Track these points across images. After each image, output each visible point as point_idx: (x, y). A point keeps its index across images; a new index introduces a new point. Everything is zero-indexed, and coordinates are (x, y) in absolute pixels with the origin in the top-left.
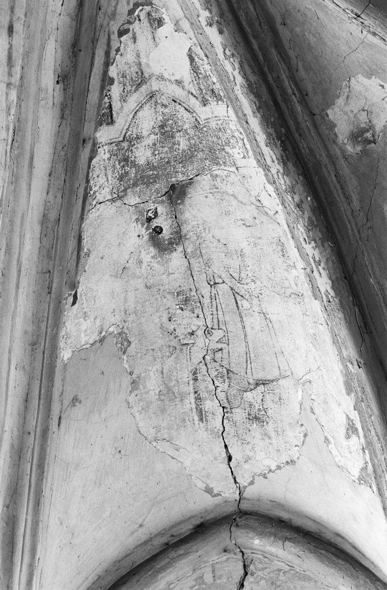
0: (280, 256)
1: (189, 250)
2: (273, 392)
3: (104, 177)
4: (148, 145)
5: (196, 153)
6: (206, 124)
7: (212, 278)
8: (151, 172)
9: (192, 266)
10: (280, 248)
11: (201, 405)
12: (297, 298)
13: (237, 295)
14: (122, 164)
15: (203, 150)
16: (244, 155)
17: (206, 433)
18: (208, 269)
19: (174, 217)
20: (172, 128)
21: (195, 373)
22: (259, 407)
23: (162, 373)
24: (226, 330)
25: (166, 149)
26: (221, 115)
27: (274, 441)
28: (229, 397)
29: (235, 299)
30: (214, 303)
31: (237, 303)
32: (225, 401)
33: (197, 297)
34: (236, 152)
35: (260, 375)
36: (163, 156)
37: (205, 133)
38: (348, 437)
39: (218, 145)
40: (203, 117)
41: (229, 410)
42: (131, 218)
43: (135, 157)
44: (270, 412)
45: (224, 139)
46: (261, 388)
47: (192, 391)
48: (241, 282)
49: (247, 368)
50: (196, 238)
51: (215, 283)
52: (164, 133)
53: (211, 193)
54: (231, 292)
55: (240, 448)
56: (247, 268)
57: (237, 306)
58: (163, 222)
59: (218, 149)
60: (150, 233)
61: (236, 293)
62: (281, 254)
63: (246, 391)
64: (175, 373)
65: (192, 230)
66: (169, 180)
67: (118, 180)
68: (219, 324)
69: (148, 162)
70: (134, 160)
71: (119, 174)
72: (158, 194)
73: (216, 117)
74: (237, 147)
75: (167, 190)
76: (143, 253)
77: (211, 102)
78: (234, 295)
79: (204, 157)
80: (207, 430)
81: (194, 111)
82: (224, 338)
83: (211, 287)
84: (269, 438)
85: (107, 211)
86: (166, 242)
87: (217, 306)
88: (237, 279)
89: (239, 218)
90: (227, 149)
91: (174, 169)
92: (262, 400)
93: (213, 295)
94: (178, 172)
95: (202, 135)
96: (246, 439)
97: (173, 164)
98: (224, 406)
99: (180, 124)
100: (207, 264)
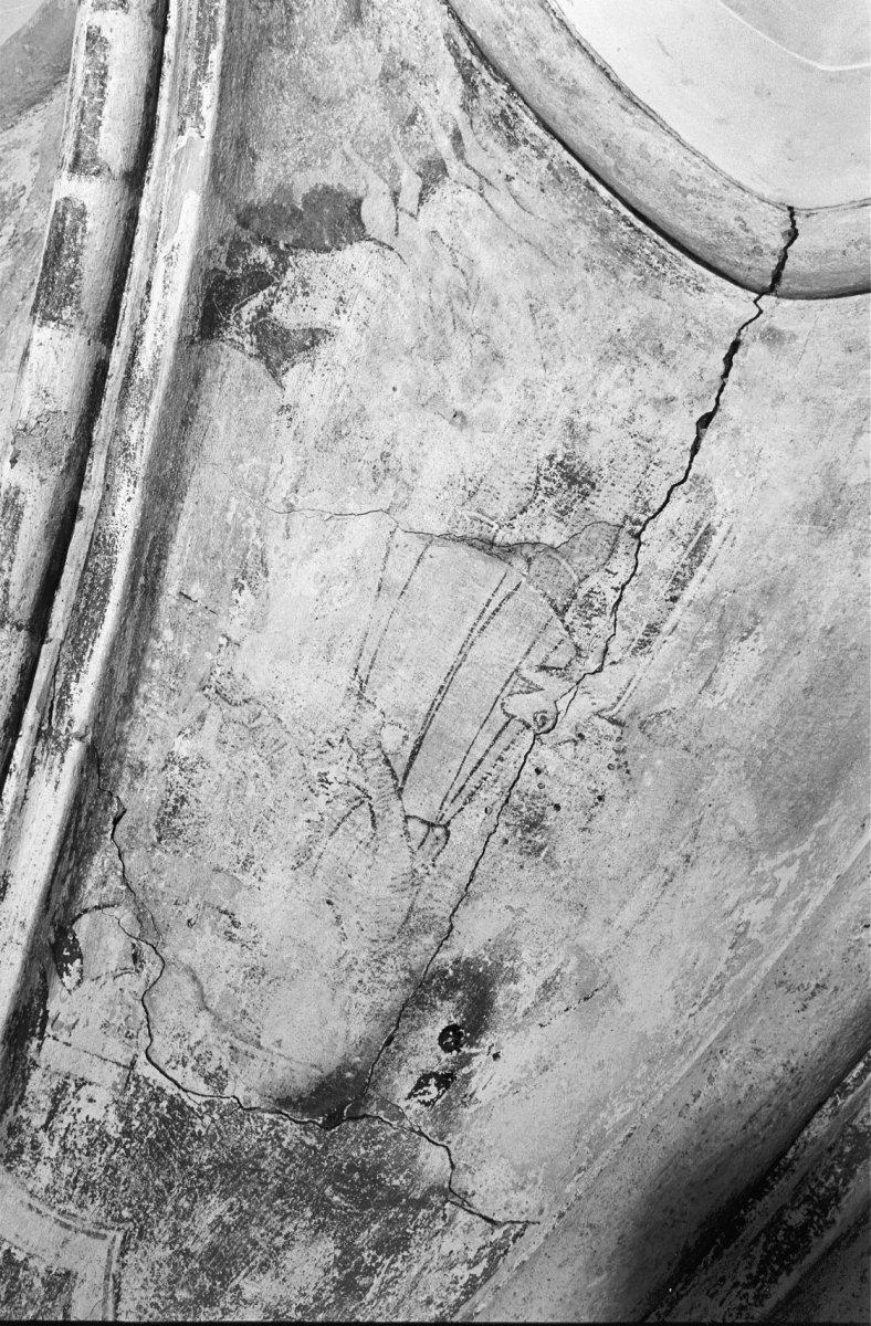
0: (194, 804)
1: (429, 940)
3: (421, 1286)
4: (277, 1276)
5: (206, 1168)
6: (109, 1223)
7: (430, 841)
8: (336, 1198)
9: (454, 901)
10: (176, 822)
13: (400, 772)
14: (363, 1282)
15: (183, 1163)
16: (79, 1087)
17: (719, 497)
19: (392, 1045)
20: (193, 1275)
21: (643, 644)
22: (546, 499)
23: (708, 683)
24: (498, 705)
25: (255, 1233)
26: (48, 1223)
27: (564, 412)
28: (606, 553)
29: (410, 765)
30: (473, 781)
31: (414, 754)
32: (621, 549)
33: (502, 817)
34: (97, 1106)
36: (274, 1221)
37: (134, 1202)
38: (315, 337)
39: (132, 1152)
40: (100, 1249)
41: (628, 526)
42: (474, 1116)
43: (327, 1271)
45: (100, 1159)
47: (678, 606)
49: (508, 597)
50: (390, 961)
51: (431, 825)
52: (220, 1278)
53: (259, 1046)
54: (406, 787)
55: (664, 432)
56: (316, 817)
57: (419, 746)
58: (425, 1051)
59: (141, 1142)
60: (471, 1044)
61: (394, 777)
62: (185, 806)
63: (552, 547)
64: (686, 665)
65: (379, 986)
66: (320, 1147)
67: (406, 1248)
68: (503, 729)
69: (316, 1232)
70: (335, 1265)
71: (393, 1262)
72: (375, 1132)
73: (68, 1227)
74: (81, 1117)
75: (351, 1124)
76: (525, 1003)
77: (42, 1269)
78: (406, 775)
80: (713, 504)
81: (107, 1277)
82: (516, 690)
83: (449, 823)
85: (490, 1184)
86: (460, 994)
87: (471, 774)
88: (365, 809)
89: (237, 946)
90: (114, 1127)
91: (287, 1166)
92: (524, 510)
93: (459, 803)
94: (285, 1150)
95: (145, 1203)
97: (275, 1182)
98: (633, 540)
99: (167, 1270)
100: (413, 880)
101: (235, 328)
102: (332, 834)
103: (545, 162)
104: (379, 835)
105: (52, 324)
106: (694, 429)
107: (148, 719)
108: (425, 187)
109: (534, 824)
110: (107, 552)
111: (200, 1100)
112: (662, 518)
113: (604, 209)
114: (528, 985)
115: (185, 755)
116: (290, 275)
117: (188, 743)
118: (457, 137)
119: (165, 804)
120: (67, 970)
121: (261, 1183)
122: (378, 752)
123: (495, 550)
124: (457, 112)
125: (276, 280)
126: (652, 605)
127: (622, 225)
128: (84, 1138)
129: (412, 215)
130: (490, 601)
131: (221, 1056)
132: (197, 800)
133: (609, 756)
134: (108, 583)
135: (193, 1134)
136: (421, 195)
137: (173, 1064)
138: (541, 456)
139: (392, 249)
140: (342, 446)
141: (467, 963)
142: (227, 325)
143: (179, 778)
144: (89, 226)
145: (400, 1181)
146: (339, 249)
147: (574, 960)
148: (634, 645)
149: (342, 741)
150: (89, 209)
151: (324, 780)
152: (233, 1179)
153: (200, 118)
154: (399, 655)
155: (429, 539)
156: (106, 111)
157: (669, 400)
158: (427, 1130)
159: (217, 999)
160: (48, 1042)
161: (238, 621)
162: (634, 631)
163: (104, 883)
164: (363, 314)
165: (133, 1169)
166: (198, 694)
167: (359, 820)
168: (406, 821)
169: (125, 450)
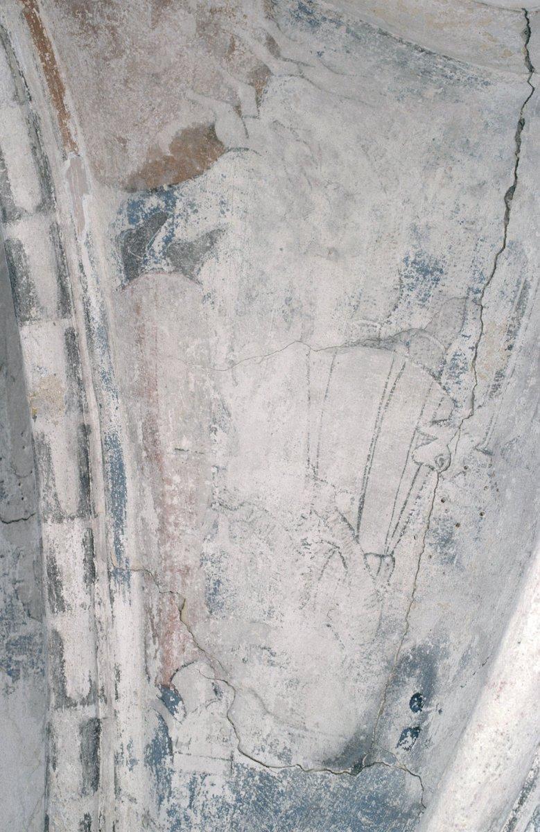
0: (226, 583)
1: (395, 637)
2: (364, 322)
5: (290, 812)
8: (363, 819)
10: (218, 598)
11: (513, 319)
12: (227, 499)
13: (354, 525)
15: (276, 812)
16: (203, 779)
18: (382, 590)
19: (384, 713)
21: (496, 387)
22: (410, 293)
24: (410, 458)
28: (460, 322)
29: (360, 517)
31: (361, 509)
32: (470, 316)
33: (426, 540)
34: (218, 787)
35: (378, 359)
38: (212, 237)
39: (245, 811)
41: (472, 296)
44: (392, 281)
45: (226, 819)
46: (386, 332)
47: (514, 353)
48: (331, 547)
50: (373, 657)
51: (382, 557)
53: (306, 730)
54: (360, 534)
56: (307, 571)
59: (248, 803)
60: (428, 705)
61: (351, 529)
63: (421, 330)
66: (351, 788)
68: (416, 475)
75: (367, 769)
76: (453, 672)
78: (358, 525)
79: (281, 799)
82: (419, 444)
83: (393, 552)
84: (414, 229)
86: (418, 671)
88: (337, 556)
90: (230, 798)
91: (335, 803)
92: (396, 307)
93: (397, 537)
94: (331, 793)
96: (463, 231)
101: (152, 261)
102: (319, 580)
103: (344, 28)
104: (350, 572)
105: (27, 322)
106: (503, 204)
107: (181, 537)
108: (258, 92)
109: (447, 541)
110: (115, 447)
111: (278, 771)
112: (493, 284)
113: (399, 45)
114: (455, 657)
115: (212, 552)
116: (179, 205)
117: (212, 545)
118: (271, 42)
119: (208, 588)
120: (175, 709)
121: (322, 816)
122: (337, 514)
123: (382, 344)
124: (266, 24)
125: (170, 213)
126: (497, 356)
127: (416, 54)
128: (215, 808)
129: (254, 117)
130: (387, 383)
131: (284, 741)
132: (227, 580)
133: (486, 480)
134: (121, 466)
135: (278, 793)
136: (257, 99)
137: (256, 752)
138: (398, 261)
139: (247, 149)
140: (256, 306)
141: (420, 649)
142: (145, 262)
143: (212, 569)
144: (27, 252)
145: (397, 803)
146: (208, 168)
147: (477, 638)
148: (490, 390)
149: (311, 513)
150: (23, 243)
151: (305, 544)
152: (307, 816)
153: (74, 144)
154: (335, 442)
155: (334, 351)
156: (10, 176)
157: (482, 185)
158: (409, 766)
159: (273, 706)
160: (177, 756)
161: (219, 454)
162: (488, 379)
163: (184, 650)
164: (242, 206)
165: (247, 821)
166: (209, 510)
167: (335, 564)
168: (365, 558)
169: (104, 377)
